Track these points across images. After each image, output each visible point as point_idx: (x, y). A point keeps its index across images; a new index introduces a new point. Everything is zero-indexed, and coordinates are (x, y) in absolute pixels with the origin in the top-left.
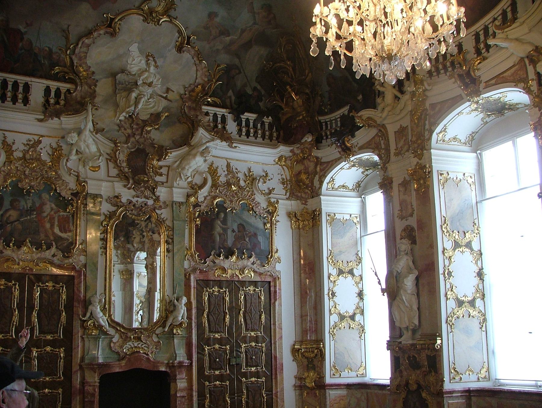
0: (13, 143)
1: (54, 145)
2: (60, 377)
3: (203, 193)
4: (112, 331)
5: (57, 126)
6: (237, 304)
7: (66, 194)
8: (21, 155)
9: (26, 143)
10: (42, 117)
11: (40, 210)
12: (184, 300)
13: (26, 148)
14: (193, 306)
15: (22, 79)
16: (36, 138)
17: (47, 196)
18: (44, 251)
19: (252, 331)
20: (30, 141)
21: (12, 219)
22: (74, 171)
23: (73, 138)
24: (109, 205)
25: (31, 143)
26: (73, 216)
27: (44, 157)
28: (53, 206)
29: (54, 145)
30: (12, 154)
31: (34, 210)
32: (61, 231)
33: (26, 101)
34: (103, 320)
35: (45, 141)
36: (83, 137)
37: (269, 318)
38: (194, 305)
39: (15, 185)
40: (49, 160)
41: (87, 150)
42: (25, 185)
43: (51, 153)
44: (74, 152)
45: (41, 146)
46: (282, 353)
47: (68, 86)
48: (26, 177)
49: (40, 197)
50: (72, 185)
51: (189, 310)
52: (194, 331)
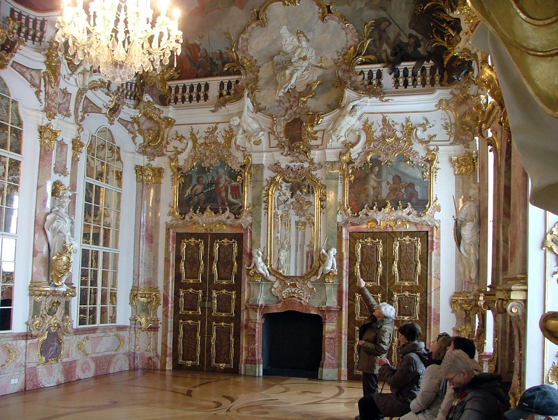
0: (198, 133)
1: (227, 129)
2: (232, 314)
3: (355, 152)
4: (272, 278)
5: (226, 113)
6: (391, 254)
7: (236, 167)
9: (206, 131)
10: (214, 108)
11: (217, 183)
12: (333, 251)
13: (207, 135)
14: (345, 257)
15: (203, 81)
16: (214, 125)
17: (223, 171)
18: (221, 215)
19: (407, 280)
20: (209, 128)
21: (198, 192)
22: (242, 147)
23: (236, 121)
24: (271, 172)
25: (210, 130)
26: (242, 184)
27: (220, 140)
28: (227, 177)
29: (227, 129)
30: (196, 142)
31: (213, 184)
32: (233, 198)
33: (206, 97)
34: (262, 268)
35: (221, 127)
36: (243, 118)
37: (426, 268)
38: (346, 254)
39: (199, 165)
40: (223, 142)
41: (250, 129)
42: (206, 164)
43: (224, 136)
44: (241, 131)
45: (217, 131)
46: (439, 304)
47: (236, 77)
49: (217, 172)
50: (241, 160)
51: (340, 260)
52: (344, 280)
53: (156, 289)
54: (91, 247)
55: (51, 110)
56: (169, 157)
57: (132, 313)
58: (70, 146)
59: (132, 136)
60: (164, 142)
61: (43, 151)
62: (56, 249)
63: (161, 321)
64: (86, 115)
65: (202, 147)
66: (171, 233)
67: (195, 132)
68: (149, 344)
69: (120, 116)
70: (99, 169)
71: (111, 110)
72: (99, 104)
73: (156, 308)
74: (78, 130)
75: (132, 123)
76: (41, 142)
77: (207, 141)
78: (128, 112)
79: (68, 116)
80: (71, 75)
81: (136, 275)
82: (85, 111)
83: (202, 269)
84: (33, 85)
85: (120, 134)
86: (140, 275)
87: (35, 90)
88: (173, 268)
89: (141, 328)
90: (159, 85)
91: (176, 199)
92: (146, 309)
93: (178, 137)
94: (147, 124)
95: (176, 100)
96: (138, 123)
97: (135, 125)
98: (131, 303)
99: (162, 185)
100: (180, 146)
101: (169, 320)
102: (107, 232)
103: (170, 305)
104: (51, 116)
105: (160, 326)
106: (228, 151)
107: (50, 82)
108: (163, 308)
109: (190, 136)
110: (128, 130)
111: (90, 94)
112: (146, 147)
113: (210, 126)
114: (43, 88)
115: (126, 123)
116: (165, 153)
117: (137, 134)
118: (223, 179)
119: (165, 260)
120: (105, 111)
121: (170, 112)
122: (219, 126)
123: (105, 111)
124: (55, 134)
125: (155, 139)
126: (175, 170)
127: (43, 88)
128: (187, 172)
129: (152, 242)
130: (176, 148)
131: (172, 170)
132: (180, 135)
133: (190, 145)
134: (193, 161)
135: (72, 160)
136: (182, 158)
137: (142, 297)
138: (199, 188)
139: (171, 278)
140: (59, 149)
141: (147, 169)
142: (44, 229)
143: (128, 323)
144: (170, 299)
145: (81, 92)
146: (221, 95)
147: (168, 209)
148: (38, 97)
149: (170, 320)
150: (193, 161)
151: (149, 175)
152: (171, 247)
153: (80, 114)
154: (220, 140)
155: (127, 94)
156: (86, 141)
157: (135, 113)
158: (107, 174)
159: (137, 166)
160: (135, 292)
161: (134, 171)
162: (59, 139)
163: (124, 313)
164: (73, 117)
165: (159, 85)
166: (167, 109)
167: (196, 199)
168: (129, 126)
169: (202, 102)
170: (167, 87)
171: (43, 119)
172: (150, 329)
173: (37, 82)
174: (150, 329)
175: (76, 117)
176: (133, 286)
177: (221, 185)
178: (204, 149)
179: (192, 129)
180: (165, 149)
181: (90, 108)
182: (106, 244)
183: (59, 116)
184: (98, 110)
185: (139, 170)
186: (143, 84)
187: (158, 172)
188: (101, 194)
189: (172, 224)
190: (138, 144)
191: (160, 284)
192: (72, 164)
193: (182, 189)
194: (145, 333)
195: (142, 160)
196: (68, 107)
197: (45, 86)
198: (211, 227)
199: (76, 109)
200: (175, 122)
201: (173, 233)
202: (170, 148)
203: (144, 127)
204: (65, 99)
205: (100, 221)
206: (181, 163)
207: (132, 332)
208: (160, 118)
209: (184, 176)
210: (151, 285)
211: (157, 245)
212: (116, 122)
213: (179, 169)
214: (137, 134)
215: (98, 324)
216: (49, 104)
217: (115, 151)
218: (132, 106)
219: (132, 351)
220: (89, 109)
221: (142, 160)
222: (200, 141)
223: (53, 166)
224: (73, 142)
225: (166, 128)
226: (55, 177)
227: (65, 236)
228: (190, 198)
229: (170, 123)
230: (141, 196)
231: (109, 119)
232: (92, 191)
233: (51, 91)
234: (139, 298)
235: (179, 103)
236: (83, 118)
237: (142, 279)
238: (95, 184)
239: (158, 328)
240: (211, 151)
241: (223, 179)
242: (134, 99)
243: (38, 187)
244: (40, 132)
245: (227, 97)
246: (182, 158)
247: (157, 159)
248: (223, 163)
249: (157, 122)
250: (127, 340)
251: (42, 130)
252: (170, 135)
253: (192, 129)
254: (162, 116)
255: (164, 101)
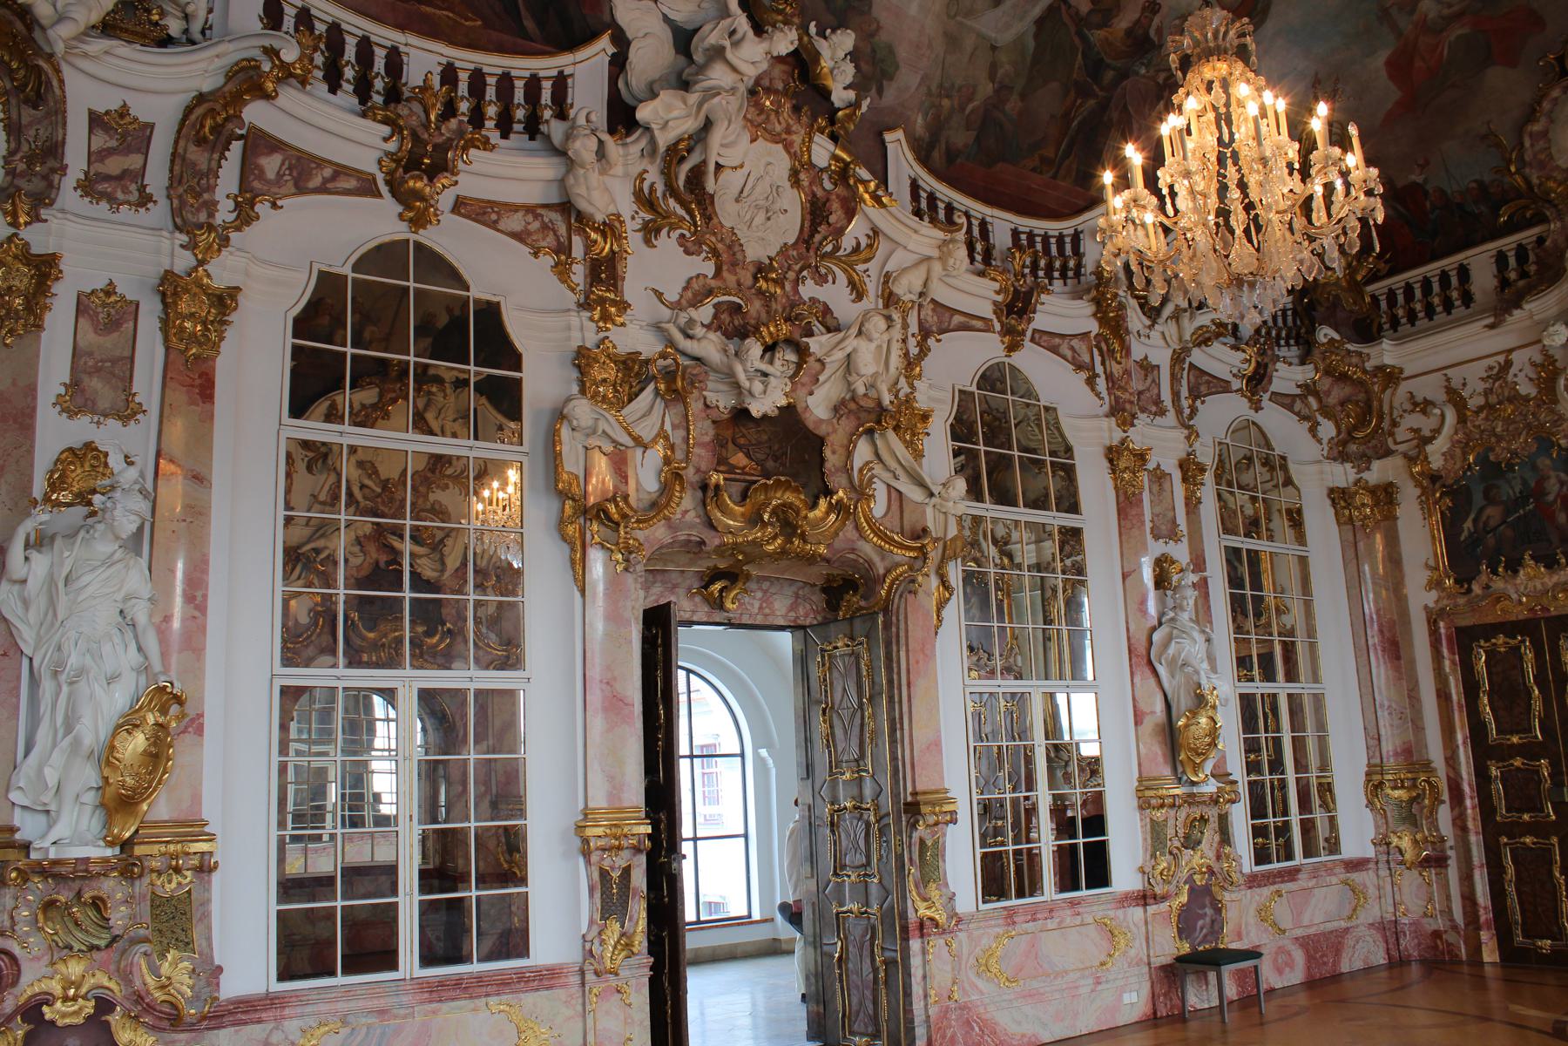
0: (1464, 385)
1: (1538, 358)
8: (1481, 401)
11: (1539, 492)
15: (1449, 263)
16: (1501, 359)
17: (1548, 462)
20: (1491, 368)
21: (1493, 523)
27: (1526, 388)
29: (1538, 358)
30: (1465, 406)
33: (1467, 299)
39: (1483, 460)
40: (1533, 392)
42: (1500, 453)
43: (1533, 376)
45: (1513, 370)
48: (1499, 439)
49: (1534, 467)
53: (1427, 766)
54: (1259, 688)
55: (1124, 410)
56: (1405, 455)
57: (1377, 827)
58: (1177, 476)
59: (1307, 425)
60: (1386, 425)
61: (1122, 498)
62: (1183, 702)
63: (1450, 842)
64: (1198, 403)
65: (1483, 415)
66: (1443, 631)
67: (1456, 383)
68: (1430, 900)
69: (1273, 388)
70: (1249, 511)
71: (1250, 380)
72: (1221, 371)
73: (1433, 811)
74: (1188, 438)
75: (1303, 397)
76: (1115, 479)
77: (1493, 399)
78: (1289, 375)
79: (1162, 412)
80: (1151, 327)
81: (1374, 738)
82: (1195, 394)
83: (1537, 706)
84: (1079, 367)
85: (1281, 426)
86: (1383, 739)
87: (1084, 375)
88: (1461, 711)
89: (1402, 863)
90: (1348, 301)
91: (1441, 549)
92: (1411, 815)
93: (1416, 404)
94: (1337, 393)
95: (1395, 323)
96: (1316, 394)
97: (1311, 400)
98: (1370, 804)
99: (1400, 523)
100: (1426, 424)
101: (1473, 838)
102: (1289, 650)
103: (1468, 803)
104: (1127, 422)
105: (1450, 853)
106: (1552, 411)
107: (1112, 352)
108: (1452, 809)
109: (1444, 397)
110: (1297, 414)
111: (1198, 357)
112: (1344, 443)
113: (1491, 361)
114: (1099, 369)
115: (1287, 401)
116: (1393, 447)
117: (1320, 418)
118: (1553, 481)
119: (1439, 696)
120: (1236, 384)
121: (1387, 353)
122: (1514, 356)
123: (1236, 384)
124: (1141, 457)
125: (1362, 422)
126: (1425, 483)
127: (1099, 369)
128: (1457, 481)
129: (1398, 658)
130: (1417, 431)
131: (1418, 484)
132: (1419, 399)
133: (1451, 417)
134: (1465, 455)
135: (1187, 505)
136: (1437, 452)
137: (1395, 788)
138: (1493, 513)
139: (1459, 737)
140: (1155, 488)
141: (1356, 493)
142: (1150, 663)
143: (1370, 852)
144: (1466, 788)
145: (1178, 358)
146: (1504, 283)
147: (1423, 576)
148: (1093, 389)
149: (1475, 840)
150: (1465, 455)
151: (1363, 505)
152: (1447, 663)
153: (1185, 403)
154: (1526, 388)
155: (1278, 336)
156: (1206, 455)
157: (1305, 373)
158: (1269, 520)
159: (1331, 491)
160: (1377, 778)
161: (1329, 502)
162: (1151, 466)
163: (1357, 829)
164: (1171, 414)
165: (1348, 301)
166: (1377, 348)
167: (1490, 540)
168: (1298, 405)
169: (1459, 311)
170: (1368, 299)
171: (1110, 430)
172: (1426, 863)
173: (1086, 358)
174: (1426, 863)
175: (1179, 412)
176: (1369, 765)
177: (1551, 498)
178: (1486, 419)
179: (1448, 380)
180: (1390, 440)
181: (1206, 385)
182: (1291, 676)
183: (1142, 418)
184: (1224, 387)
185: (1339, 497)
186: (1312, 306)
187: (1385, 495)
188: (1263, 566)
189: (1443, 610)
190: (1325, 441)
191: (1436, 754)
192: (1188, 513)
193: (1451, 527)
194: (1415, 872)
195: (1343, 475)
196: (1159, 395)
197: (1103, 363)
198: (1545, 602)
199: (1176, 395)
200: (1401, 371)
201: (1447, 628)
202: (1402, 433)
203: (1332, 400)
204: (1149, 380)
205: (1269, 624)
206: (1436, 463)
207: (1384, 872)
208: (1365, 371)
209: (1450, 492)
210: (1413, 759)
211: (1412, 662)
212: (1265, 402)
213: (1434, 478)
214: (1320, 418)
215: (1299, 859)
216: (1117, 399)
217: (1277, 466)
218: (1296, 361)
219: (1389, 917)
220: (1203, 389)
221: (1343, 475)
222: (1474, 403)
223: (1148, 525)
224: (1181, 466)
225: (1383, 391)
226: (1157, 548)
227: (1197, 672)
228: (1476, 540)
229: (1391, 376)
230: (1353, 555)
231: (1250, 400)
232: (1241, 562)
233: (1117, 369)
234: (1389, 791)
235: (1405, 328)
236: (1194, 411)
237: (1388, 747)
238: (1245, 547)
239: (1446, 858)
240: (1508, 421)
241: (1553, 481)
242: (1297, 344)
243: (1125, 576)
244: (1111, 461)
245: (1521, 283)
246: (1437, 452)
247: (1376, 465)
248: (1545, 442)
249: (1361, 383)
250: (1372, 891)
251: (1112, 454)
252: (1396, 404)
253: (1448, 380)
254: (1369, 366)
255: (1366, 331)
